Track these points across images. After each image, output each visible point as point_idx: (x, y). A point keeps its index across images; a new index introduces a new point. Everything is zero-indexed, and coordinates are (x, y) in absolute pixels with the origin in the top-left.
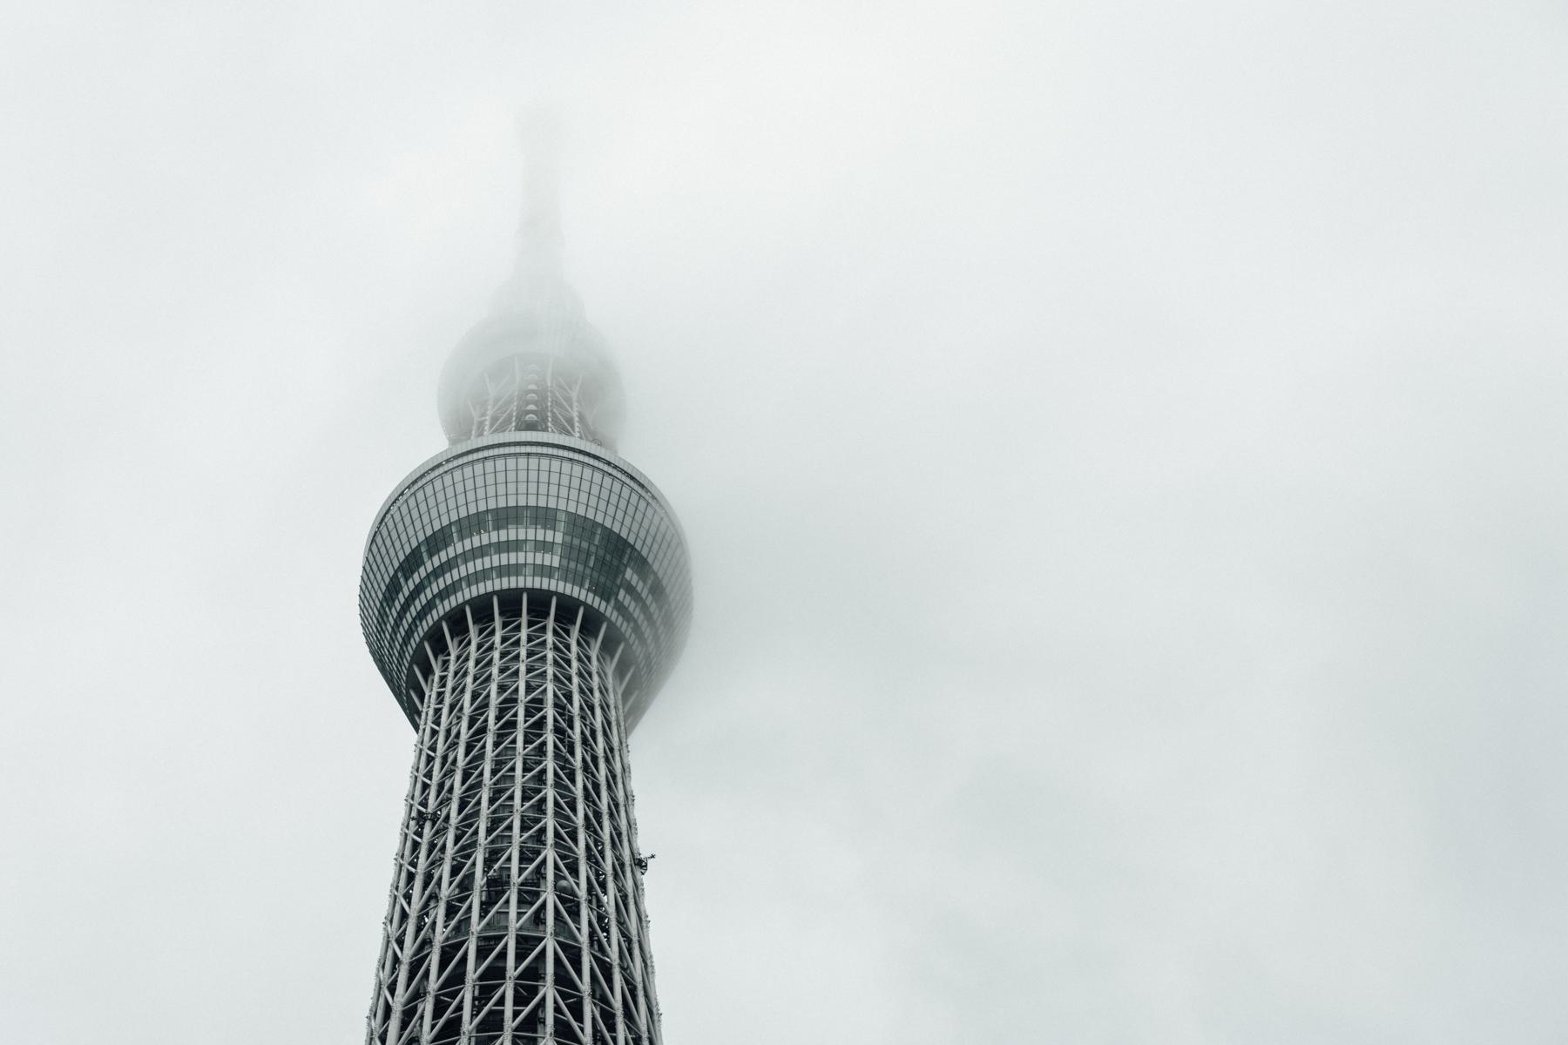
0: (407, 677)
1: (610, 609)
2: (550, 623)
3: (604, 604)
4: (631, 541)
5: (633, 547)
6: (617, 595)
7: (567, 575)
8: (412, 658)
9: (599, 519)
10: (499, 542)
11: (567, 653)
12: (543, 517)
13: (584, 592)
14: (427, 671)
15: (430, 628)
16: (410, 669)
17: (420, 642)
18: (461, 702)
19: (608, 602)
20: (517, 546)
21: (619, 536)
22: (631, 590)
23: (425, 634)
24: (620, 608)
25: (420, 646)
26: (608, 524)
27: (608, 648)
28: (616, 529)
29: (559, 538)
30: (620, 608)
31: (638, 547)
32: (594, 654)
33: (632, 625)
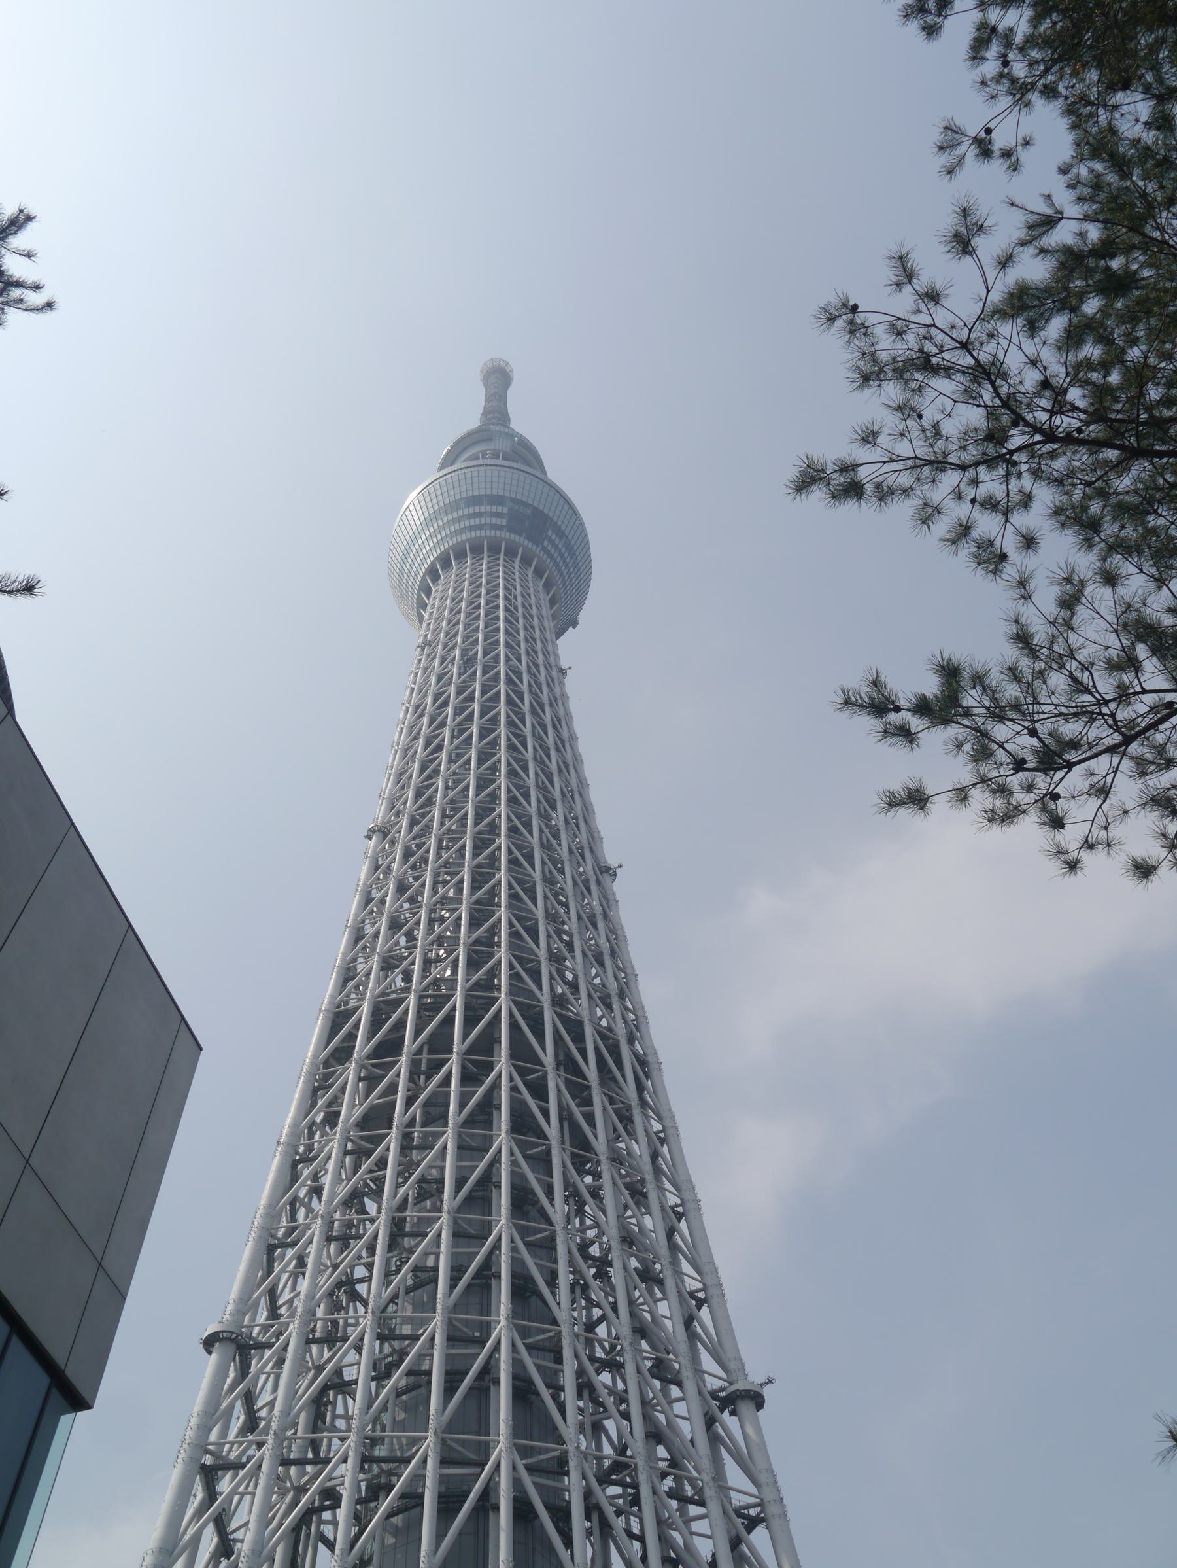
0: (417, 599)
1: (538, 551)
2: (502, 556)
3: (535, 547)
4: (551, 515)
5: (552, 519)
7: (511, 530)
9: (530, 502)
12: (497, 500)
13: (522, 539)
14: (428, 592)
16: (418, 594)
19: (537, 546)
20: (480, 515)
21: (542, 512)
22: (552, 542)
23: (426, 570)
24: (545, 549)
25: (423, 578)
26: (536, 505)
27: (538, 573)
28: (541, 507)
29: (506, 510)
30: (545, 549)
31: (555, 519)
32: (530, 578)
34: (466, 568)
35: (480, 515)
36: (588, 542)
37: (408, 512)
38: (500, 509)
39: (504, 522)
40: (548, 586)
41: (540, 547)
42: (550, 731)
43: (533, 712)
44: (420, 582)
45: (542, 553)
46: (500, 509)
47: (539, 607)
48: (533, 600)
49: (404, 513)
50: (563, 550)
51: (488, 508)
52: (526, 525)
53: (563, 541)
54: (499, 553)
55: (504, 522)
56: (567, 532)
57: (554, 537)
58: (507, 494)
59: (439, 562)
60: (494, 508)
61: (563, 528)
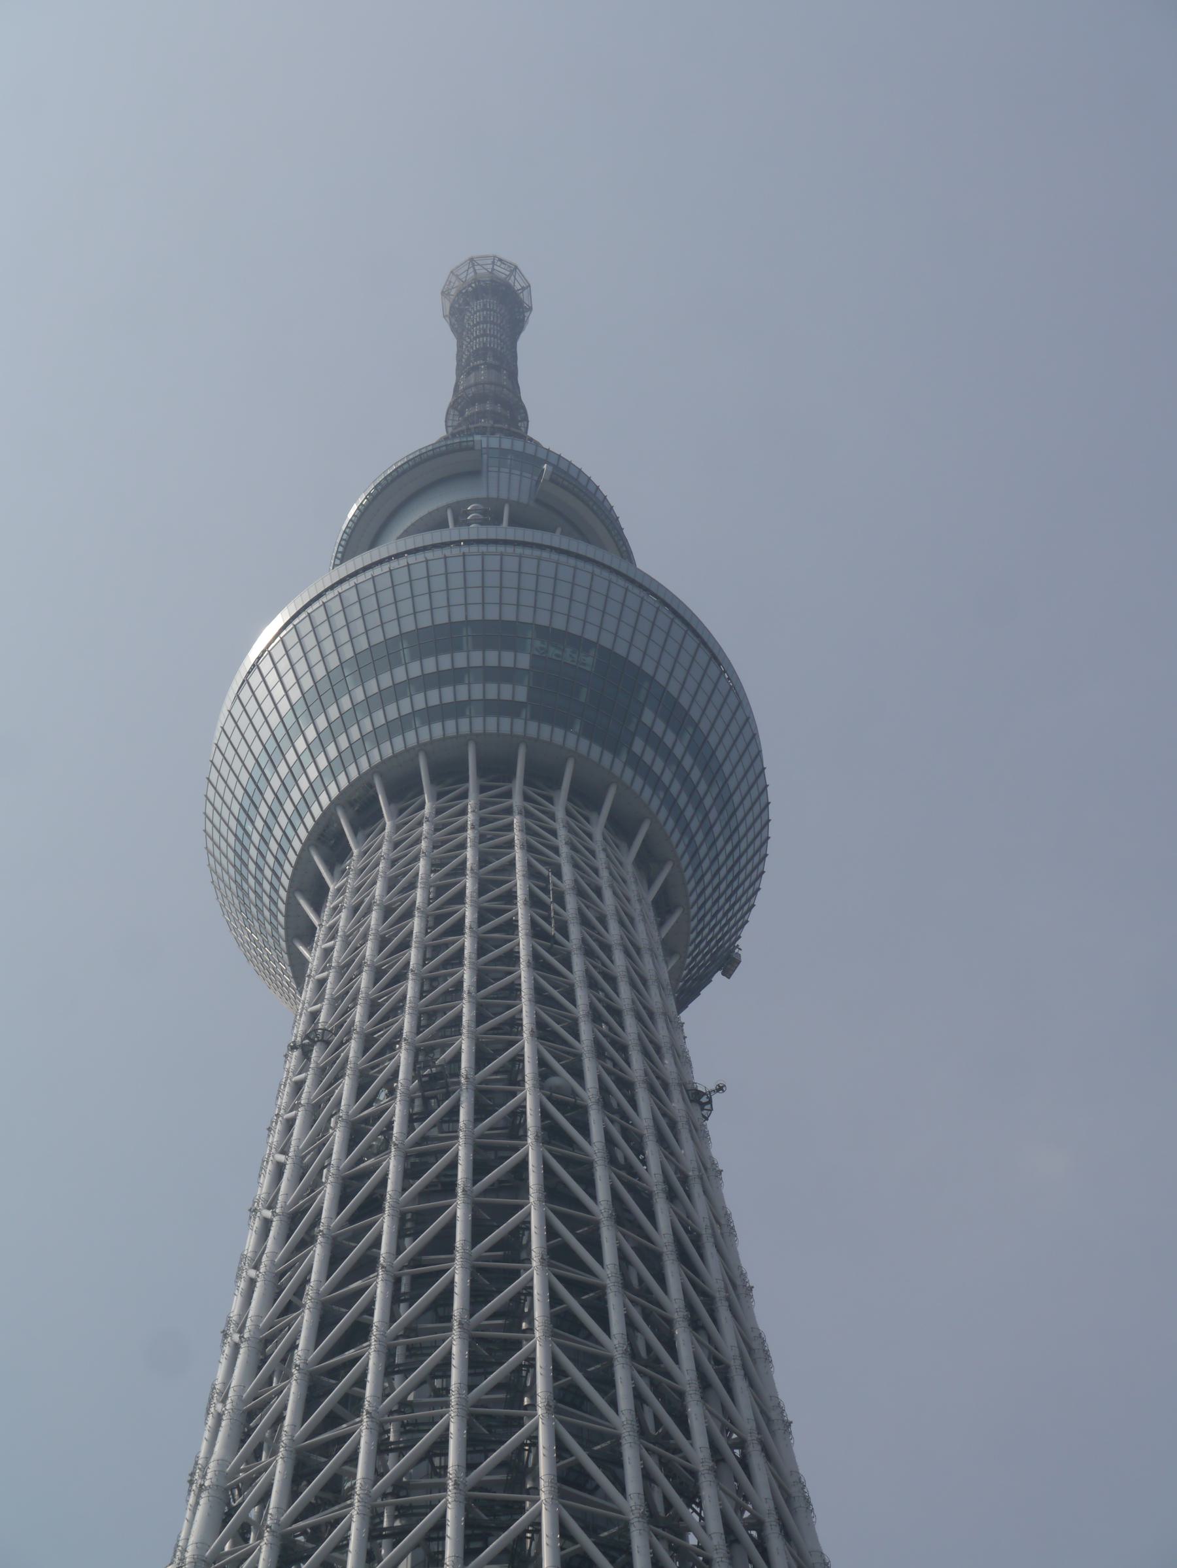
0: (286, 916)
2: (518, 786)
3: (608, 757)
6: (631, 744)
8: (291, 880)
10: (424, 675)
11: (552, 822)
15: (317, 823)
17: (302, 850)
18: (373, 892)
19: (616, 753)
20: (455, 676)
23: (310, 834)
24: (635, 762)
25: (303, 856)
29: (524, 661)
30: (635, 762)
32: (598, 844)
33: (662, 795)
34: (420, 824)
35: (455, 676)
36: (755, 736)
37: (255, 679)
38: (508, 659)
39: (522, 694)
40: (647, 863)
41: (624, 756)
42: (673, 1270)
43: (622, 1217)
44: (295, 868)
45: (629, 773)
46: (508, 659)
47: (626, 922)
48: (609, 903)
49: (246, 681)
50: (688, 762)
51: (476, 659)
52: (583, 698)
53: (687, 737)
54: (510, 777)
55: (522, 694)
56: (695, 713)
57: (659, 727)
58: (526, 617)
59: (346, 812)
60: (492, 658)
61: (685, 700)
